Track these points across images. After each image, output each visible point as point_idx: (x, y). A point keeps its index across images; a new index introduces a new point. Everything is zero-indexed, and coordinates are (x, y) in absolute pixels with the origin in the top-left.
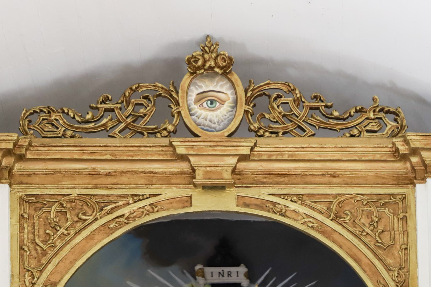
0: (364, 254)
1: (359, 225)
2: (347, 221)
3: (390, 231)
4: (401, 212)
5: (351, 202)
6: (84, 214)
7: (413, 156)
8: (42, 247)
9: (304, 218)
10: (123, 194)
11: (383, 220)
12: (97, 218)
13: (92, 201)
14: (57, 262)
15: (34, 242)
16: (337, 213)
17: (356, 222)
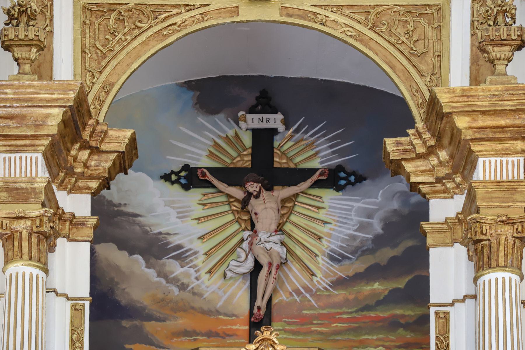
0: (398, 61)
1: (395, 34)
2: (384, 31)
3: (424, 39)
4: (436, 21)
6: (140, 22)
8: (102, 50)
9: (342, 28)
10: (176, 4)
11: (418, 30)
12: (152, 25)
13: (148, 10)
14: (115, 65)
15: (94, 46)
16: (375, 23)
17: (392, 31)
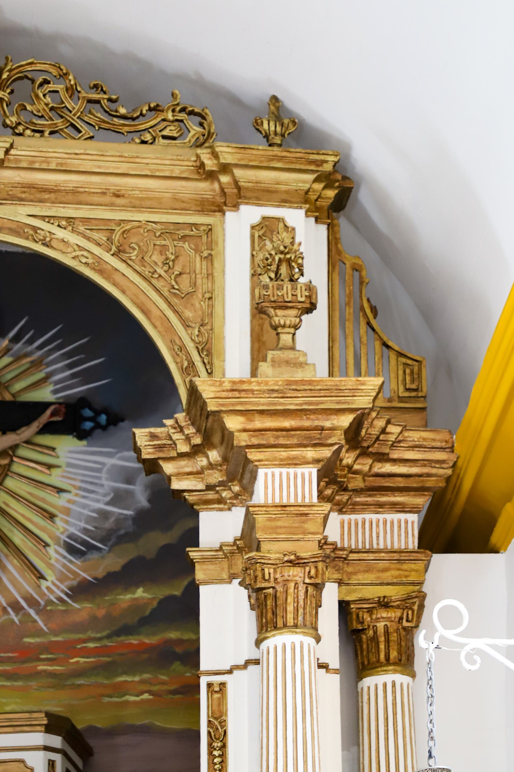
5: (140, 232)
7: (223, 174)
